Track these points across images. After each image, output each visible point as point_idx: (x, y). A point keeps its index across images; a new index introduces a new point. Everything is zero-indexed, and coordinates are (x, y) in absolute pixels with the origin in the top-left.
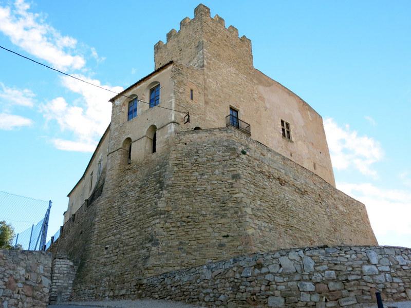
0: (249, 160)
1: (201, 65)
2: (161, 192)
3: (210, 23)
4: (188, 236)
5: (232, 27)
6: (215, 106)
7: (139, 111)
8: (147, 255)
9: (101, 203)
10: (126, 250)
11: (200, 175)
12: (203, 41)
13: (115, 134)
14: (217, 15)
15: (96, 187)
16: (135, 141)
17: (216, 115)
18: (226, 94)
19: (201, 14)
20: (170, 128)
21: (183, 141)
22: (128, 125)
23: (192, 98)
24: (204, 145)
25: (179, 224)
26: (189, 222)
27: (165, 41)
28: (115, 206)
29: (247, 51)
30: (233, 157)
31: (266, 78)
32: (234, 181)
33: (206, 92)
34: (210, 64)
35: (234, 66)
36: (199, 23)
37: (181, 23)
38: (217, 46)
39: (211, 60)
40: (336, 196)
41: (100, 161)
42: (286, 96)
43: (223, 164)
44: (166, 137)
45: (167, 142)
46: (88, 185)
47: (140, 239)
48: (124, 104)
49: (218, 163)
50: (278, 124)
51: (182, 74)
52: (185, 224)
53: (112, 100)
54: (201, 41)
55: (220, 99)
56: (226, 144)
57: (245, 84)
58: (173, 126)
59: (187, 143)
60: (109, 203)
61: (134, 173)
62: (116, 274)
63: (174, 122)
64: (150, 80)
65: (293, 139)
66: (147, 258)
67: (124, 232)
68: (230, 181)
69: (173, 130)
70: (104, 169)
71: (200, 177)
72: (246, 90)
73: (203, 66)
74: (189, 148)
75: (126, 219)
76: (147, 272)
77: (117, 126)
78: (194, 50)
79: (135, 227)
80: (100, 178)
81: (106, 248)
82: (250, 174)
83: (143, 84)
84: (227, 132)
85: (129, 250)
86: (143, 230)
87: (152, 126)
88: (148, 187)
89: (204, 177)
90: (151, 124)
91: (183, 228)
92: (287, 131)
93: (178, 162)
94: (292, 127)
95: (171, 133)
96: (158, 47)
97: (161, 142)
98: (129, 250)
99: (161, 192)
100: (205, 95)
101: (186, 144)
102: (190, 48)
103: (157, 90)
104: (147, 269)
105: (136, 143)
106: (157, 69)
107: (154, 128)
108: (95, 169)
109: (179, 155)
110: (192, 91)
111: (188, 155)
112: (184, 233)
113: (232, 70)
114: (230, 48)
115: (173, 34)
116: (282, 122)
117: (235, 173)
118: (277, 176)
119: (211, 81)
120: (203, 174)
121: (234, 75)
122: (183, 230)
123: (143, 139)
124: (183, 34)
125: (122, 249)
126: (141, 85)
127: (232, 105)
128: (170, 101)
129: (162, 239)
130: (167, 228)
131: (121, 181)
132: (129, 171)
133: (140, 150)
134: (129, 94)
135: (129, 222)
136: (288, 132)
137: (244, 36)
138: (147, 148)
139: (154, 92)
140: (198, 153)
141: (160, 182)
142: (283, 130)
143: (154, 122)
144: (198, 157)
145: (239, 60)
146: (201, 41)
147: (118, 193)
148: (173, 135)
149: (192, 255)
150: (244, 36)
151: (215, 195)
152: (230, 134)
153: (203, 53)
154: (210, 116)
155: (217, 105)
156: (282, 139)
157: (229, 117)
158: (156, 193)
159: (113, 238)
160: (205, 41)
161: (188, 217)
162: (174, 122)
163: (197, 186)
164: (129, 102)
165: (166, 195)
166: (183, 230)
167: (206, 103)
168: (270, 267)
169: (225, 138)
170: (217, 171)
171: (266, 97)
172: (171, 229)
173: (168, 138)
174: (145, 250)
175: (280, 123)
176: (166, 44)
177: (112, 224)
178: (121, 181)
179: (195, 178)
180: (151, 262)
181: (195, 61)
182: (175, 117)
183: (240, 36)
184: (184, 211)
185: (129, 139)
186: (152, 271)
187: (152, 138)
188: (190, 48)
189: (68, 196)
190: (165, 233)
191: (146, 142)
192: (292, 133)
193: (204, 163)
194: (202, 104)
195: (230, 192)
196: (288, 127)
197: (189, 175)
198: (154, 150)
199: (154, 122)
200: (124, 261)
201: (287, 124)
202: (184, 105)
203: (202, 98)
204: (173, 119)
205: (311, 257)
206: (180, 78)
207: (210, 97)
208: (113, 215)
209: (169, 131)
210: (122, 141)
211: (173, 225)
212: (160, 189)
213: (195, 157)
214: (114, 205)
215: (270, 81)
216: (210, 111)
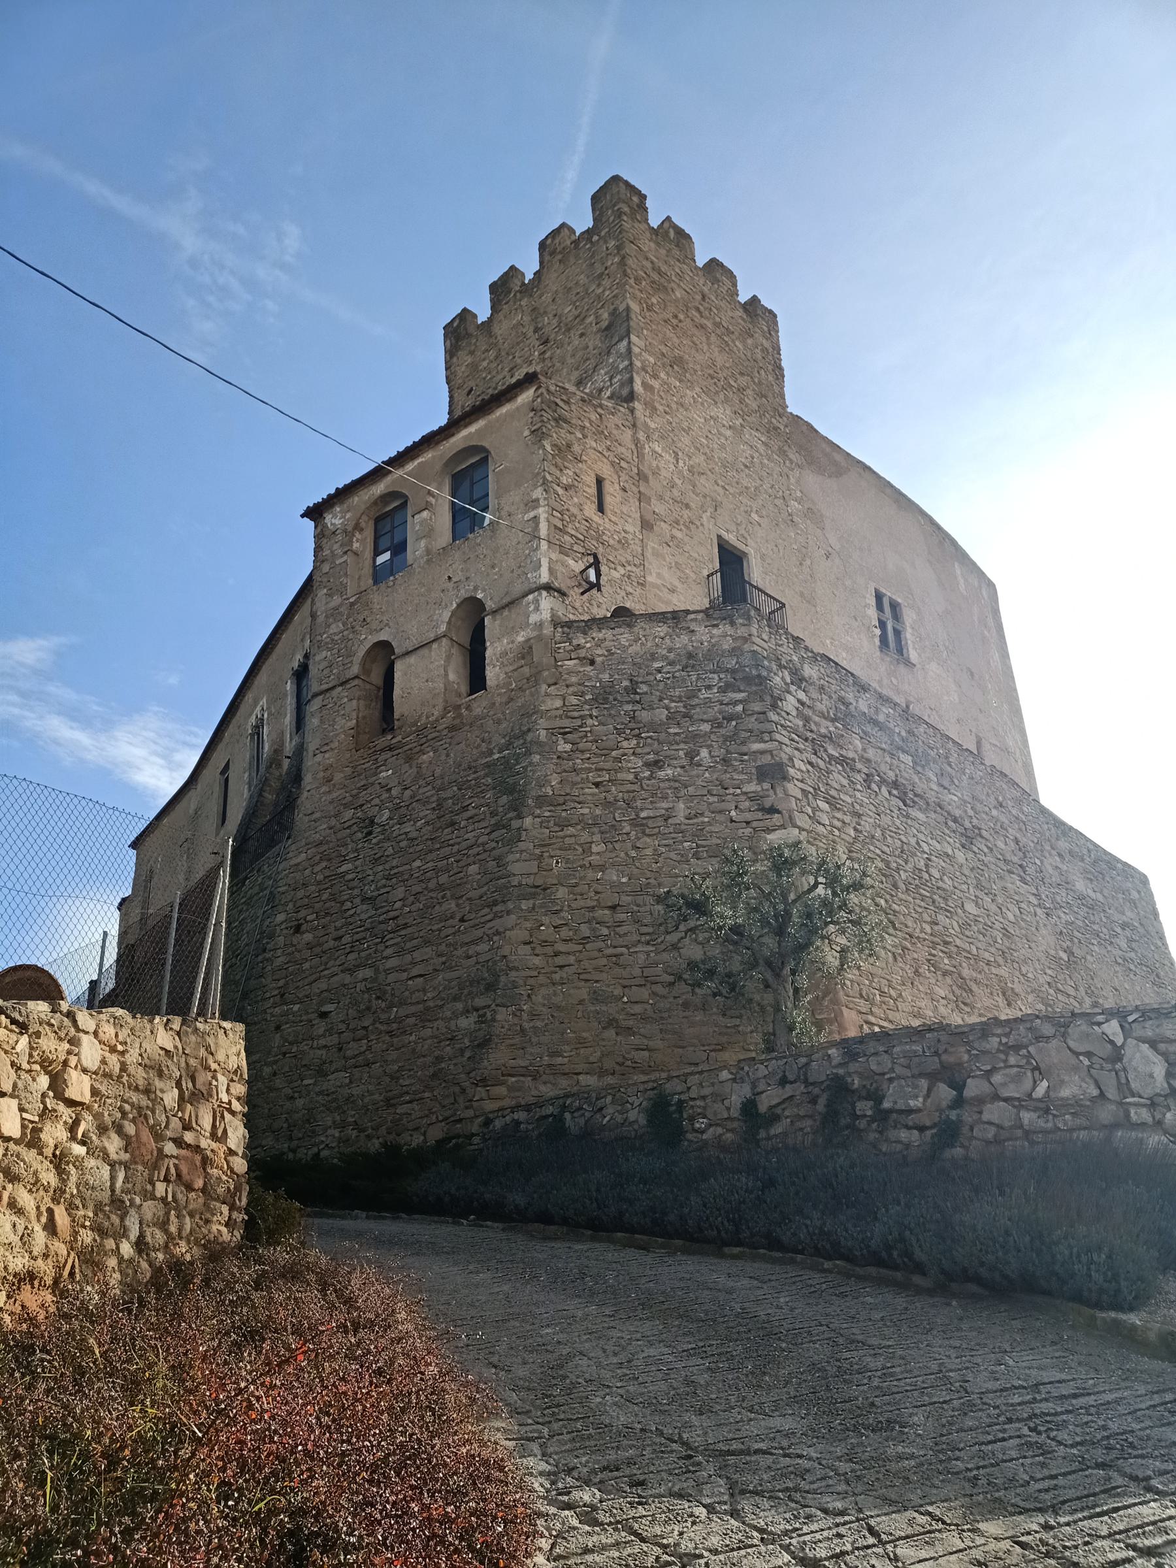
0: (807, 720)
1: (625, 392)
2: (515, 824)
3: (647, 245)
4: (617, 971)
5: (714, 264)
6: (673, 537)
7: (416, 550)
8: (481, 1034)
9: (292, 862)
10: (399, 1020)
11: (647, 765)
12: (628, 309)
13: (334, 629)
14: (668, 218)
15: (251, 814)
16: (408, 653)
18: (705, 496)
19: (620, 214)
20: (537, 609)
21: (582, 653)
22: (376, 598)
23: (601, 508)
24: (657, 665)
25: (585, 930)
26: (620, 924)
27: (483, 313)
28: (347, 872)
29: (765, 350)
30: (757, 707)
32: (766, 786)
35: (727, 400)
36: (612, 244)
37: (542, 246)
38: (674, 328)
39: (655, 376)
40: (1063, 845)
43: (723, 731)
44: (520, 639)
45: (526, 652)
46: (214, 807)
47: (450, 981)
48: (357, 527)
49: (706, 727)
50: (867, 606)
51: (566, 421)
52: (605, 931)
53: (315, 513)
54: (622, 308)
55: (686, 513)
56: (732, 663)
58: (547, 604)
59: (599, 660)
60: (324, 864)
61: (409, 759)
62: (366, 1100)
63: (548, 587)
64: (453, 440)
65: (913, 656)
66: (485, 1043)
67: (387, 958)
68: (752, 787)
69: (546, 615)
70: (276, 751)
71: (647, 774)
74: (605, 677)
75: (392, 914)
76: (484, 1095)
77: (336, 600)
78: (594, 341)
79: (427, 943)
80: (265, 782)
81: (324, 1015)
82: (810, 763)
83: (427, 456)
84: (732, 624)
85: (412, 1020)
86: (460, 952)
87: (466, 599)
88: (465, 809)
89: (661, 774)
90: (463, 594)
91: (602, 944)
92: (895, 630)
93: (566, 723)
94: (909, 616)
95: (540, 625)
96: (459, 332)
97: (505, 654)
98: (412, 1020)
99: (515, 824)
100: (641, 497)
101: (592, 663)
102: (582, 335)
103: (477, 476)
104: (483, 1082)
105: (412, 660)
106: (458, 413)
107: (474, 614)
108: (239, 753)
109: (574, 700)
110: (599, 482)
111: (603, 697)
112: (604, 961)
113: (723, 413)
114: (713, 338)
115: (516, 286)
116: (879, 597)
117: (766, 759)
118: (891, 775)
119: (659, 450)
120: (657, 764)
121: (728, 433)
122: (600, 950)
123: (435, 646)
124: (553, 282)
125: (383, 1016)
126: (420, 460)
128: (532, 514)
129: (531, 981)
130: (544, 943)
131: (364, 787)
132: (390, 754)
133: (427, 680)
134: (379, 488)
135: (406, 926)
136: (897, 633)
137: (754, 300)
138: (452, 677)
139: (467, 484)
140: (636, 693)
141: (512, 790)
142: (882, 625)
143: (476, 589)
144: (638, 707)
145: (743, 381)
146: (622, 308)
147: (355, 828)
148: (548, 630)
149: (634, 1034)
150: (754, 300)
151: (699, 833)
152: (742, 631)
153: (629, 351)
154: (659, 573)
155: (679, 535)
156: (878, 653)
157: (717, 579)
158: (497, 827)
159: (348, 979)
160: (635, 307)
161: (613, 908)
162: (548, 587)
163: (639, 803)
164: (378, 520)
165: (534, 833)
166: (600, 950)
167: (646, 525)
168: (997, 1078)
169: (727, 644)
170: (704, 753)
172: (561, 947)
173: (528, 640)
174: (473, 1018)
175: (873, 601)
176: (490, 319)
177: (340, 933)
178: (364, 787)
179: (631, 777)
180: (498, 1057)
181: (601, 377)
182: (551, 571)
183: (743, 298)
184: (600, 888)
185: (385, 646)
186: (502, 1090)
187: (466, 641)
188: (582, 335)
189: (134, 845)
190: (537, 961)
191: (448, 658)
192: (909, 635)
193: (653, 727)
194: (633, 528)
195: (755, 824)
196: (897, 616)
197: (608, 765)
198: (477, 680)
199: (476, 589)
200: (393, 1055)
201: (894, 606)
202: (577, 529)
203: (633, 507)
204: (545, 577)
205: (1153, 1044)
206: (560, 435)
207: (659, 508)
208: (342, 903)
209: (534, 618)
210: (361, 653)
211: (565, 933)
212: (512, 814)
213: (629, 707)
214: (344, 868)
215: (838, 457)
216: (656, 554)
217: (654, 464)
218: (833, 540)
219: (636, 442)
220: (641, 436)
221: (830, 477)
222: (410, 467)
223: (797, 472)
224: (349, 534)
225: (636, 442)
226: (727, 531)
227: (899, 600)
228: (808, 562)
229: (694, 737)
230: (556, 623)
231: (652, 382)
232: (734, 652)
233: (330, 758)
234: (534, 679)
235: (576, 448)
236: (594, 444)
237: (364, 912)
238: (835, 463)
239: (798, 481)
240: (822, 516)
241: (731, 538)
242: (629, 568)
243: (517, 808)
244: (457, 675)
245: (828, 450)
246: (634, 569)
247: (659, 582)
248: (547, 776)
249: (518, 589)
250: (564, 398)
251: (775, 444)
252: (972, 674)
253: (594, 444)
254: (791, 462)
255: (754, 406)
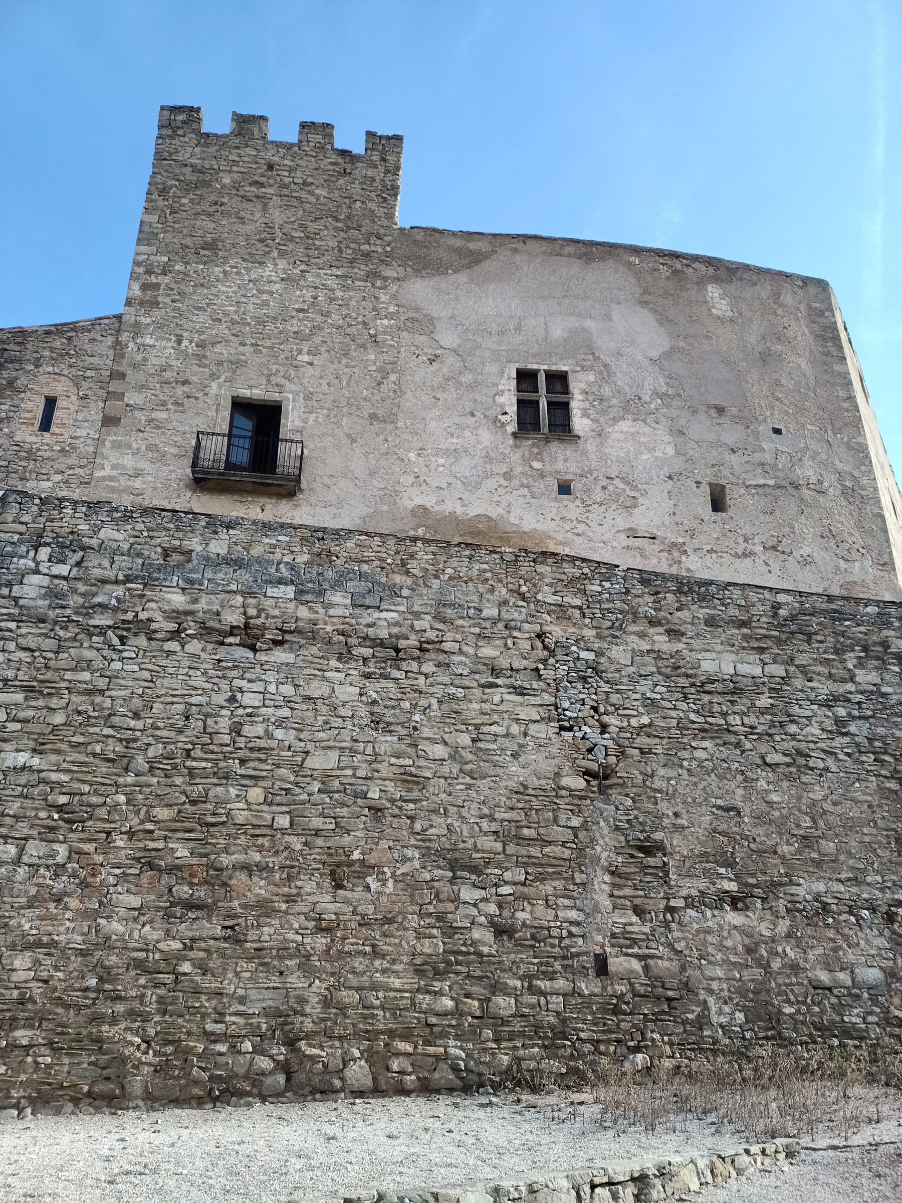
14: (234, 113)
17: (152, 448)
18: (220, 363)
31: (458, 243)
33: (114, 386)
34: (156, 286)
35: (282, 254)
38: (209, 215)
42: (570, 270)
50: (501, 393)
51: (12, 362)
57: (332, 300)
65: (579, 423)
72: (336, 319)
110: (51, 403)
116: (526, 378)
127: (246, 393)
145: (312, 227)
150: (370, 134)
156: (511, 442)
167: (110, 421)
171: (436, 311)
192: (576, 406)
207: (132, 398)
215: (473, 246)
217: (139, 358)
220: (124, 337)
221: (455, 272)
223: (394, 288)
226: (251, 387)
227: (565, 368)
228: (393, 377)
235: (22, 381)
236: (50, 369)
238: (471, 253)
239: (394, 297)
240: (431, 320)
241: (257, 393)
242: (71, 472)
245: (458, 243)
246: (77, 471)
247: (114, 473)
250: (19, 340)
251: (361, 270)
252: (721, 410)
253: (50, 369)
254: (385, 279)
255: (333, 243)
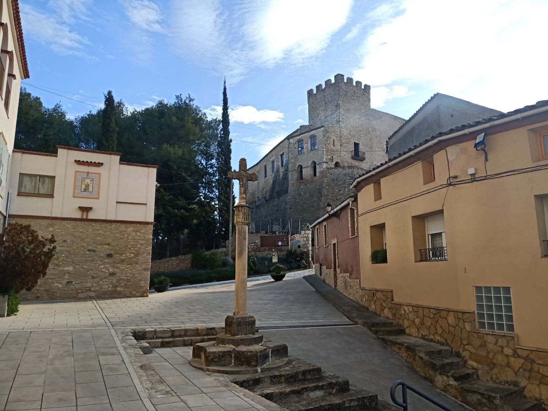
3: (344, 87)
7: (305, 150)
22: (299, 157)
41: (273, 162)
45: (322, 172)
58: (325, 165)
73: (340, 121)
78: (334, 108)
96: (310, 92)
107: (314, 163)
111: (333, 180)
120: (340, 191)
124: (327, 90)
133: (307, 172)
145: (361, 107)
157: (353, 152)
160: (341, 103)
167: (341, 145)
181: (335, 115)
206: (327, 135)
207: (343, 141)
218: (378, 134)
219: (340, 131)
222: (304, 135)
224: (294, 144)
225: (340, 131)
229: (345, 187)
230: (327, 168)
231: (344, 117)
232: (352, 174)
233: (293, 182)
234: (323, 176)
237: (300, 207)
241: (357, 142)
243: (321, 196)
244: (312, 173)
248: (325, 192)
249: (321, 161)
